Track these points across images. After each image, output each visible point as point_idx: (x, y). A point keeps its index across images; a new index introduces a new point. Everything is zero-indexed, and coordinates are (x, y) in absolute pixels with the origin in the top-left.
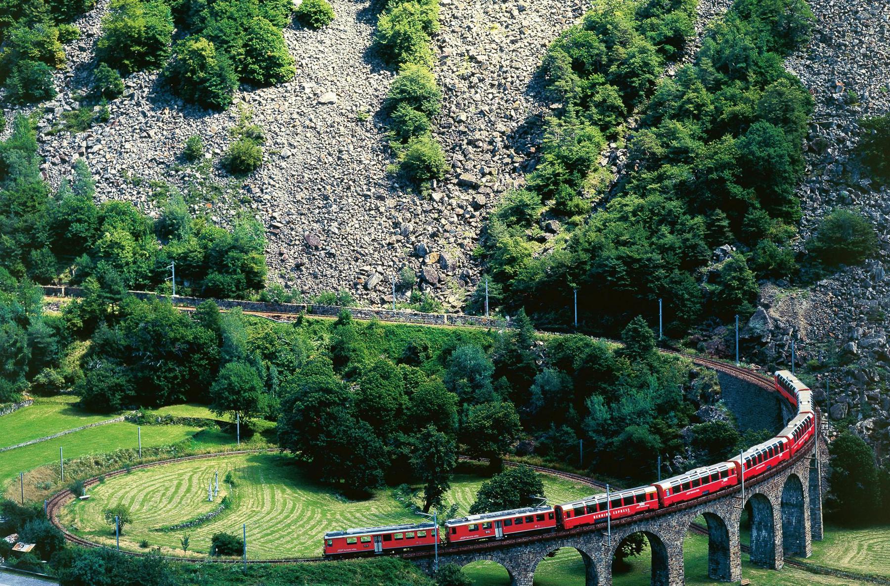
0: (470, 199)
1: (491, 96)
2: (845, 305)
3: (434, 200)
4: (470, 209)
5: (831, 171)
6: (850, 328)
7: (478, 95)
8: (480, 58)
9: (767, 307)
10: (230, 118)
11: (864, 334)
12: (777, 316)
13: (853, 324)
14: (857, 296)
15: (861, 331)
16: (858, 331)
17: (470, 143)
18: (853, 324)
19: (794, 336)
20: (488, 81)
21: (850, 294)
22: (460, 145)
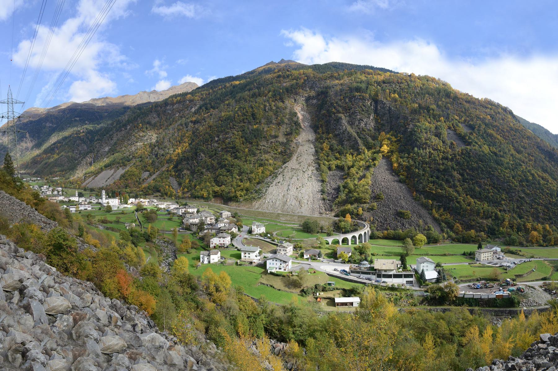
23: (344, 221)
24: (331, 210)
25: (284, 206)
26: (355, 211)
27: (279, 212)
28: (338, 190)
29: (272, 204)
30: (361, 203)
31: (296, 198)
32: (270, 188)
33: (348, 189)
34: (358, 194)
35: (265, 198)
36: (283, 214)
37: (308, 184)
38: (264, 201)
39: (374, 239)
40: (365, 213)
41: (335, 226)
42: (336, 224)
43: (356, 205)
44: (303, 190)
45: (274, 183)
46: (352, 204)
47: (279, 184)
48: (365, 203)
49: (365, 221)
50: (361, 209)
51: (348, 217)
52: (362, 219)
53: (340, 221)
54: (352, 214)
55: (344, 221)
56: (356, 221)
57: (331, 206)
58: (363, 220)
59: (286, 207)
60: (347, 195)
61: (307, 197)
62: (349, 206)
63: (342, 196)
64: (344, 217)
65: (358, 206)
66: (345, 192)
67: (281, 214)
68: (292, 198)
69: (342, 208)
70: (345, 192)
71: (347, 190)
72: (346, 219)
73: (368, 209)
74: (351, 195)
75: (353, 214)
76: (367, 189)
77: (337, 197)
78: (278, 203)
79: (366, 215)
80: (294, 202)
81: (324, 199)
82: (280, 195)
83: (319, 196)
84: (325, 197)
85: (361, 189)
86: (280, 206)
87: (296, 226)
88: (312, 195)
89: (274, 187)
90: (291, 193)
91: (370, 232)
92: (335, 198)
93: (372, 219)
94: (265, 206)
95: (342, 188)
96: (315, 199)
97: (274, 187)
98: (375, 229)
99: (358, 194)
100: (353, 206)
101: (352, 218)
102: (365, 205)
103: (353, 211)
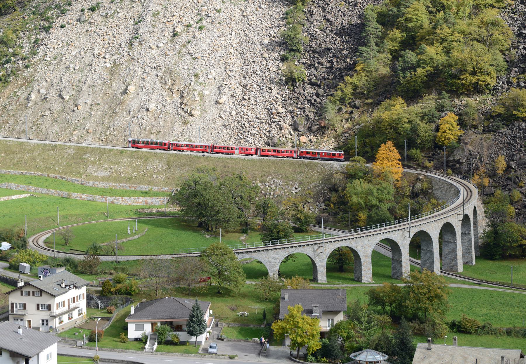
0: (315, 91)
1: (334, 39)
2: (512, 143)
3: (295, 92)
4: (315, 97)
5: (516, 72)
6: (513, 155)
7: (328, 39)
8: (331, 20)
9: (466, 144)
10: (189, 53)
11: (520, 158)
12: (471, 148)
13: (516, 153)
14: (520, 138)
15: (518, 156)
16: (516, 156)
17: (319, 63)
18: (516, 153)
19: (480, 159)
20: (334, 32)
21: (516, 137)
22: (314, 65)
23: (367, 176)
24: (322, 130)
25: (112, 114)
26: (425, 129)
27: (90, 142)
28: (356, 34)
29: (57, 106)
30: (455, 92)
31: (168, 79)
32: (55, 32)
33: (404, 29)
34: (447, 52)
35: (28, 83)
36: (103, 152)
37: (225, 15)
38: (22, 94)
39: (504, 257)
40: (472, 136)
41: (327, 200)
42: (334, 189)
43: (429, 102)
44: (202, 43)
45: (74, 12)
46: (412, 96)
47: (97, 17)
48: (477, 89)
49: (467, 175)
50: (451, 118)
51: (389, 161)
52: (454, 167)
53: (350, 176)
54: (407, 143)
55: (367, 176)
56: (423, 174)
57: (320, 111)
58: (457, 172)
59: (122, 120)
60: (396, 56)
61: (216, 73)
62: (398, 109)
63: (374, 64)
64: (372, 159)
65: (440, 109)
66: (389, 45)
67: (93, 151)
68: (150, 79)
69: (366, 119)
70: (389, 45)
71: (397, 34)
72: (375, 166)
73: (489, 116)
74: (411, 56)
75: (412, 144)
76: (494, 24)
77: (351, 68)
78: (85, 101)
79: (478, 144)
80: (158, 97)
81: (291, 81)
82: (99, 66)
83: (273, 65)
84: (298, 69)
85: (463, 25)
86: (96, 114)
87: (158, 203)
88: (238, 62)
89: (72, 30)
90: (146, 55)
91: (483, 225)
92: (340, 75)
93: (501, 163)
94: (26, 116)
95: (374, 27)
96: (253, 82)
97: (72, 30)
98: (512, 210)
99: (447, 52)
100: (417, 108)
101: (407, 161)
102: (473, 102)
103: (414, 130)
